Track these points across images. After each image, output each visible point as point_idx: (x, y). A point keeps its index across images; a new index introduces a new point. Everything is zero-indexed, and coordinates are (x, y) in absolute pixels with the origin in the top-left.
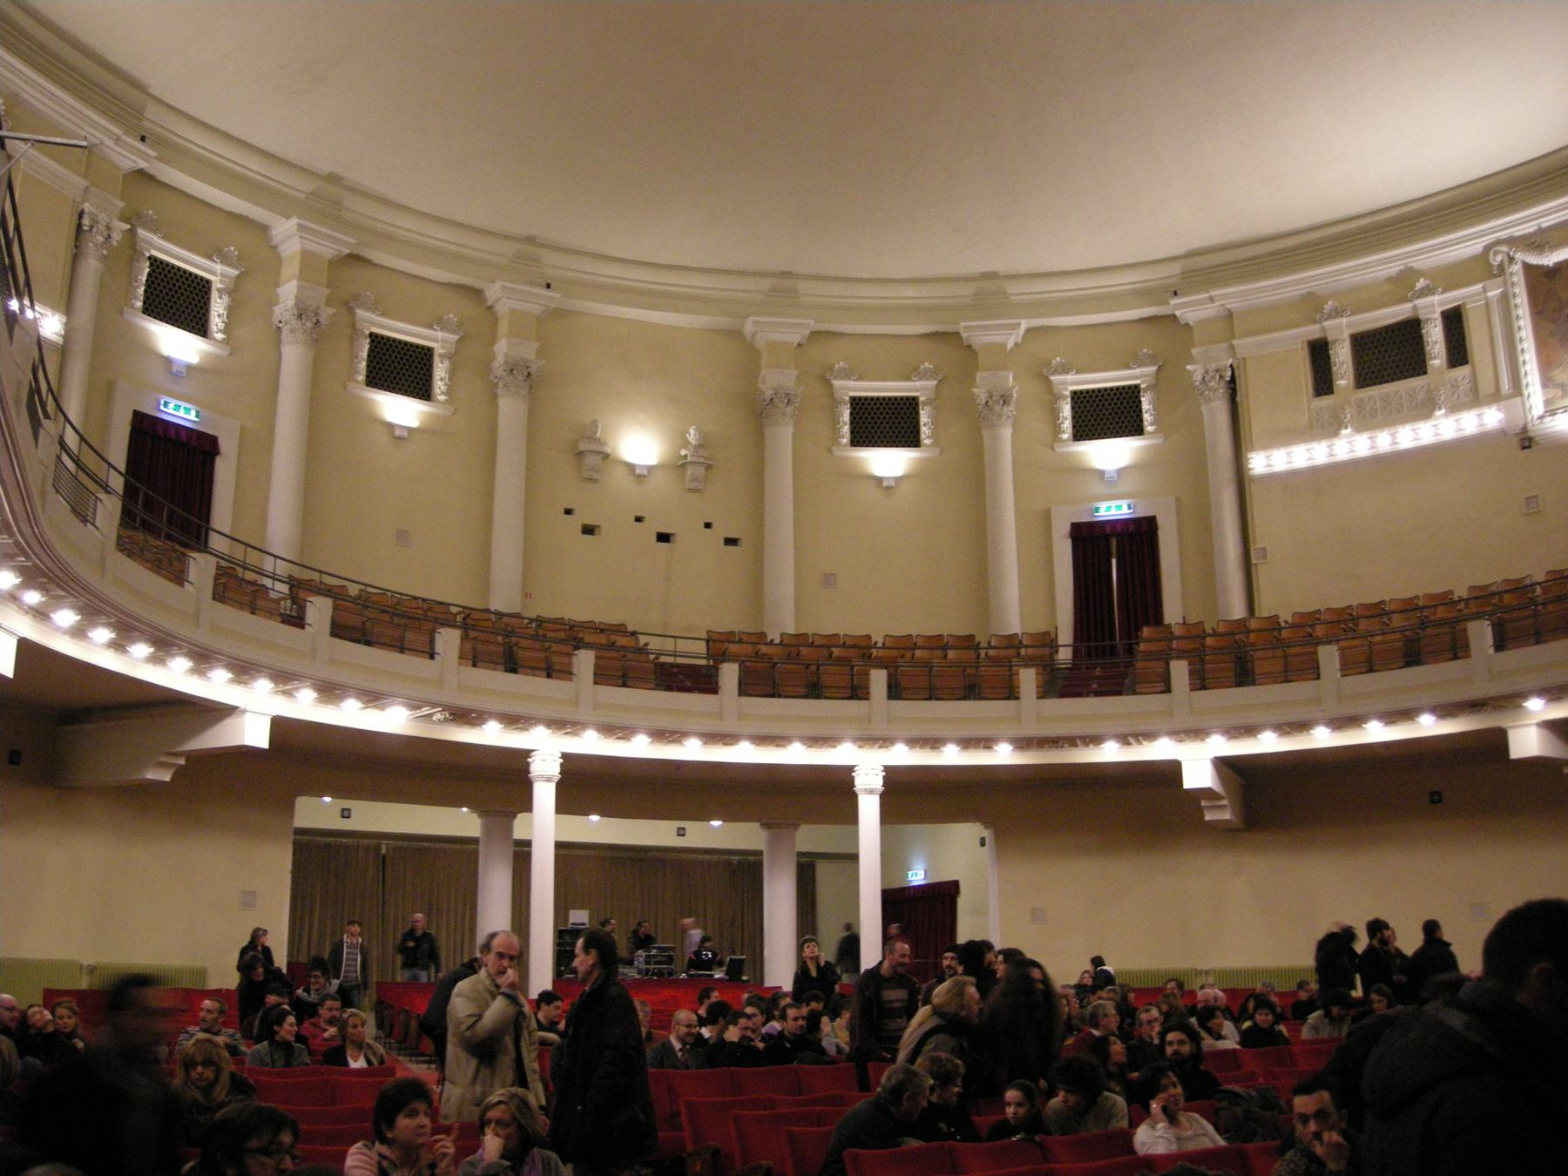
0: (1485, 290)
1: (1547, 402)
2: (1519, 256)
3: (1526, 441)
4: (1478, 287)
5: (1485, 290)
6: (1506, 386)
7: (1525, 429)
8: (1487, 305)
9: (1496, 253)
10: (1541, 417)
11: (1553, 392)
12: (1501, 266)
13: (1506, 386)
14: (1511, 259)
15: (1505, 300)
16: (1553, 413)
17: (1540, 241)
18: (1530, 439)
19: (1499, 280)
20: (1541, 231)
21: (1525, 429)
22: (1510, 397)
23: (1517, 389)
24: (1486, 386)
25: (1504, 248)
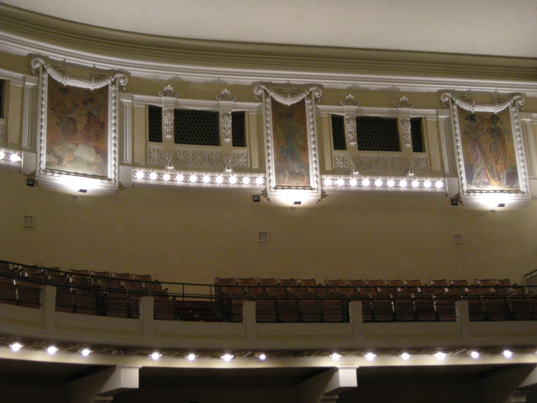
0: (24, 79)
1: (47, 163)
2: (50, 71)
3: (32, 180)
4: (21, 75)
5: (24, 79)
6: (25, 143)
7: (33, 174)
8: (23, 88)
9: (36, 62)
10: (45, 171)
11: (52, 159)
12: (37, 72)
13: (25, 143)
14: (44, 70)
15: (35, 91)
16: (52, 171)
17: (63, 68)
18: (34, 180)
19: (36, 78)
20: (64, 63)
21: (33, 174)
22: (26, 150)
23: (33, 148)
24: (13, 137)
25: (42, 61)
